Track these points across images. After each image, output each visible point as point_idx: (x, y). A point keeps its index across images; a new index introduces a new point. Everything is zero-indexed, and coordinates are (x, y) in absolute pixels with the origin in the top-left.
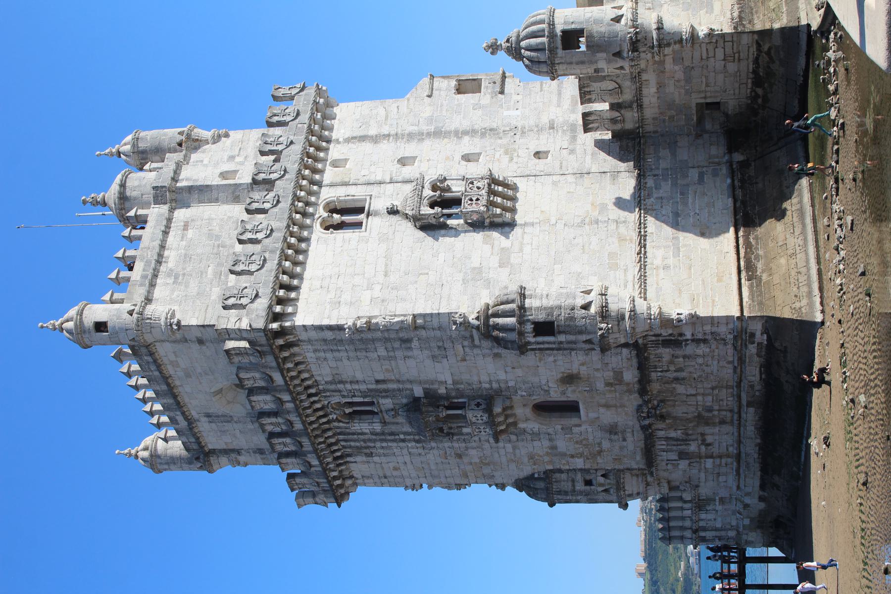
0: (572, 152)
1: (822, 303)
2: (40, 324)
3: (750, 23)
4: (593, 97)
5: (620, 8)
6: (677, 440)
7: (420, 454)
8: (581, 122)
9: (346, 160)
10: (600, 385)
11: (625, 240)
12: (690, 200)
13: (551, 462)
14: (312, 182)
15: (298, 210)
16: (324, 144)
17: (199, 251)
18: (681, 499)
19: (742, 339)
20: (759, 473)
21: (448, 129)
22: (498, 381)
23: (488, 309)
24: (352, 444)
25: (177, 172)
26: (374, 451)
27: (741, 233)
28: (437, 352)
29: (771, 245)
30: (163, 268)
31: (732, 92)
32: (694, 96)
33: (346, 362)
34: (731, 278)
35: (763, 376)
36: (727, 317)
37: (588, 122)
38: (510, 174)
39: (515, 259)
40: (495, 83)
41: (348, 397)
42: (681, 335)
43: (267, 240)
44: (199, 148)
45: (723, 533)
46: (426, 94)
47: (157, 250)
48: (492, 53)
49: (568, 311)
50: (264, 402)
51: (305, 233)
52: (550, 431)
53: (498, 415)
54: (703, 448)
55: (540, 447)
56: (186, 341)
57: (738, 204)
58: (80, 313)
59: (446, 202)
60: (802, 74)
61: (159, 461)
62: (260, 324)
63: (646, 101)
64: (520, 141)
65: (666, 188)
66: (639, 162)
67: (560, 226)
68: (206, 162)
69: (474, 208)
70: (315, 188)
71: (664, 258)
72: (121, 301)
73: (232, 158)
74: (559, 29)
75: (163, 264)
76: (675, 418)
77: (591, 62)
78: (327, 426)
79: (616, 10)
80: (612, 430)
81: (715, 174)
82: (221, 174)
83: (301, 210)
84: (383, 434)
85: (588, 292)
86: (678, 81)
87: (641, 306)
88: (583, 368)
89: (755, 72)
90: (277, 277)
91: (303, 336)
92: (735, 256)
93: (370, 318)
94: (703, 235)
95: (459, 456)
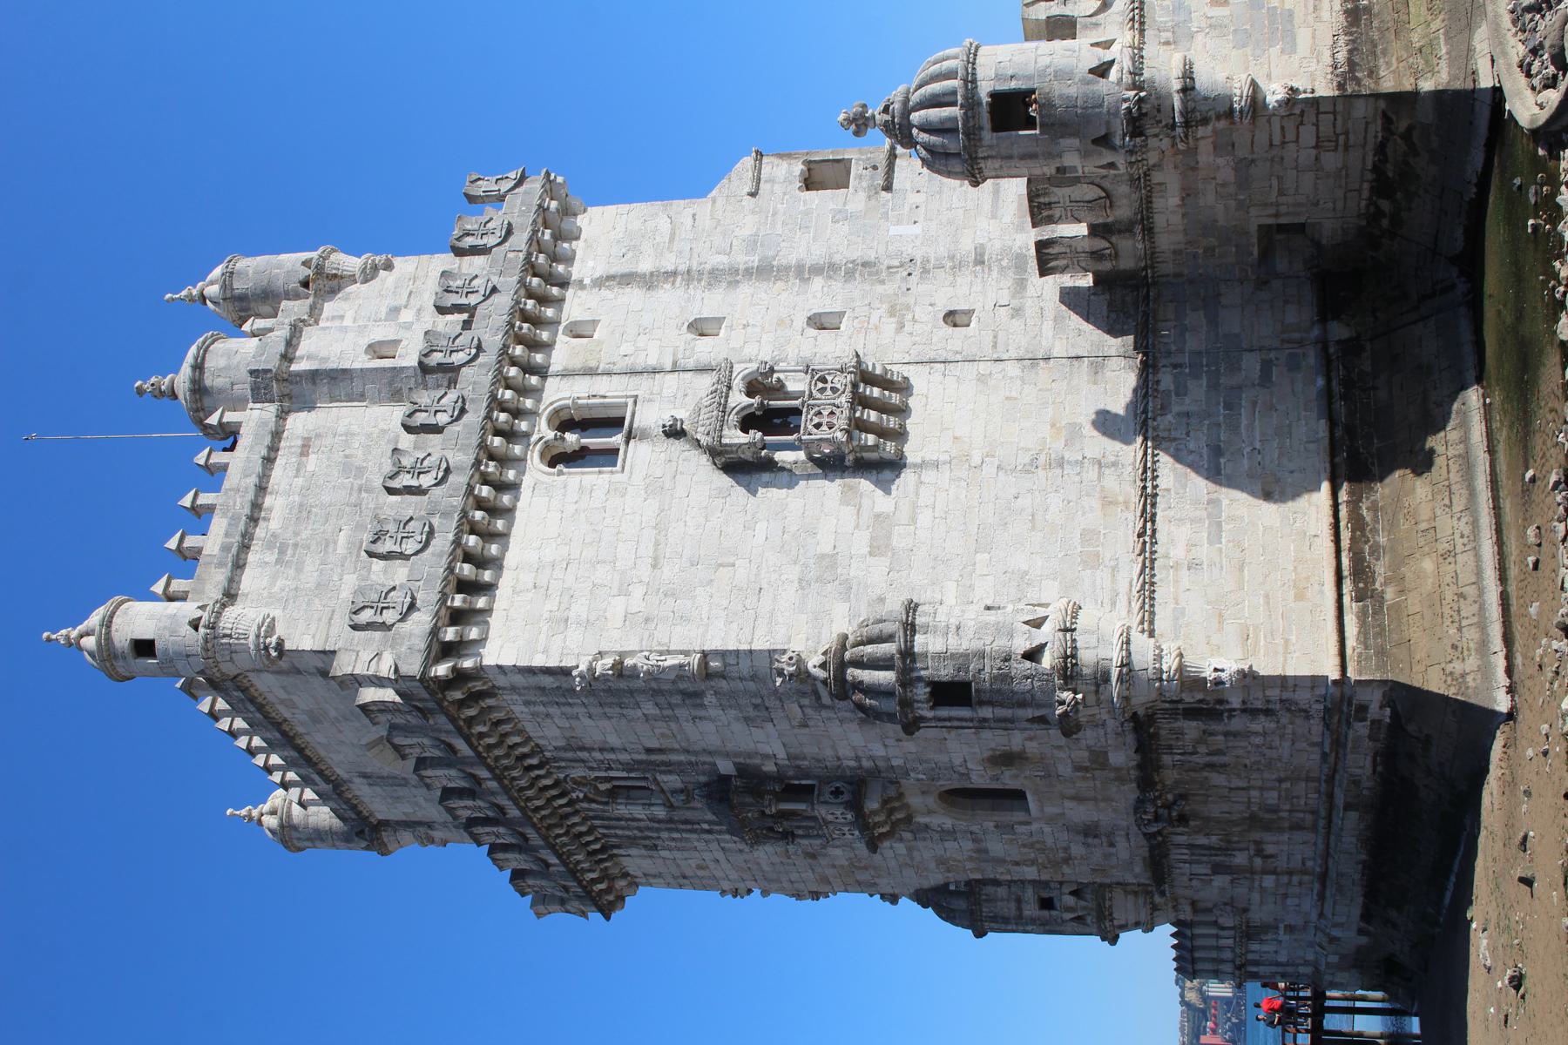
0: (1017, 312)
1: (1509, 671)
2: (45, 635)
3: (1370, 74)
4: (1057, 213)
5: (1107, 45)
6: (1210, 848)
7: (741, 851)
8: (1033, 251)
9: (595, 323)
10: (1065, 770)
11: (1114, 503)
12: (1244, 422)
13: (977, 870)
14: (529, 369)
15: (499, 426)
16: (555, 290)
18: (1215, 923)
19: (1341, 712)
20: (1360, 900)
21: (784, 262)
22: (872, 758)
23: (843, 648)
24: (620, 832)
25: (291, 343)
26: (659, 842)
27: (1343, 496)
28: (752, 713)
29: (1404, 526)
30: (260, 532)
31: (1331, 205)
32: (1253, 211)
33: (587, 722)
34: (1322, 592)
35: (1379, 769)
36: (1314, 678)
37: (1047, 258)
38: (897, 357)
39: (900, 539)
40: (875, 168)
41: (600, 769)
42: (1221, 702)
43: (437, 491)
44: (339, 289)
45: (1290, 969)
46: (747, 189)
47: (250, 496)
48: (857, 133)
49: (999, 663)
50: (449, 777)
51: (511, 475)
52: (975, 828)
53: (874, 813)
54: (1258, 861)
55: (960, 849)
56: (299, 672)
57: (1339, 433)
58: (107, 623)
59: (772, 415)
60: (1475, 180)
61: (295, 835)
62: (413, 667)
63: (1159, 221)
64: (919, 288)
65: (1198, 390)
66: (1146, 337)
67: (989, 470)
68: (348, 322)
69: (824, 433)
70: (534, 380)
71: (1191, 545)
72: (182, 597)
73: (395, 311)
74: (985, 89)
75: (261, 523)
76: (1207, 820)
77: (1050, 156)
78: (568, 810)
79: (1099, 50)
80: (1089, 832)
81: (1293, 365)
82: (370, 346)
84: (671, 821)
85: (1037, 624)
86: (1224, 185)
87: (1143, 652)
88: (1029, 744)
89: (1375, 169)
90: (450, 569)
91: (501, 681)
92: (1329, 547)
93: (623, 655)
94: (1267, 496)
95: (813, 856)
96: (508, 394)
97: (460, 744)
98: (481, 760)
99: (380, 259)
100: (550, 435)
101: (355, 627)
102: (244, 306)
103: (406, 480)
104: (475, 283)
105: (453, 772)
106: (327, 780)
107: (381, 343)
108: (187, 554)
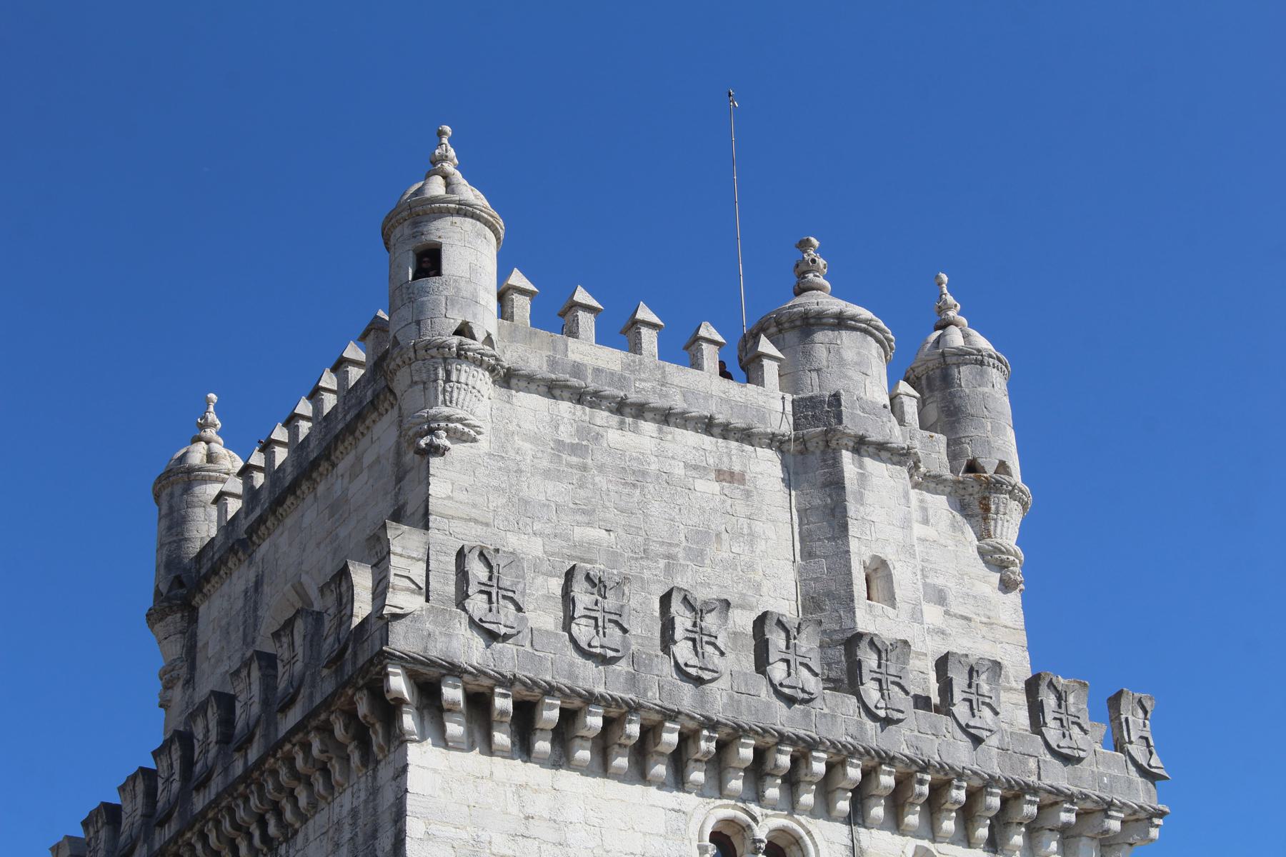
2: (447, 129)
14: (860, 796)
15: (769, 756)
16: (983, 832)
17: (655, 508)
25: (882, 450)
30: (602, 416)
43: (667, 668)
44: (968, 516)
47: (655, 401)
50: (249, 705)
51: (698, 776)
56: (399, 480)
58: (463, 210)
61: (178, 490)
62: (401, 640)
68: (918, 530)
70: (843, 805)
72: (504, 310)
75: (615, 419)
82: (884, 563)
83: (772, 763)
90: (550, 690)
91: (385, 773)
96: (819, 768)
97: (294, 716)
98: (272, 749)
99: (1016, 572)
100: (761, 833)
101: (461, 555)
102: (936, 384)
103: (683, 621)
104: (987, 712)
105: (256, 709)
106: (252, 530)
107: (889, 578)
108: (569, 317)
